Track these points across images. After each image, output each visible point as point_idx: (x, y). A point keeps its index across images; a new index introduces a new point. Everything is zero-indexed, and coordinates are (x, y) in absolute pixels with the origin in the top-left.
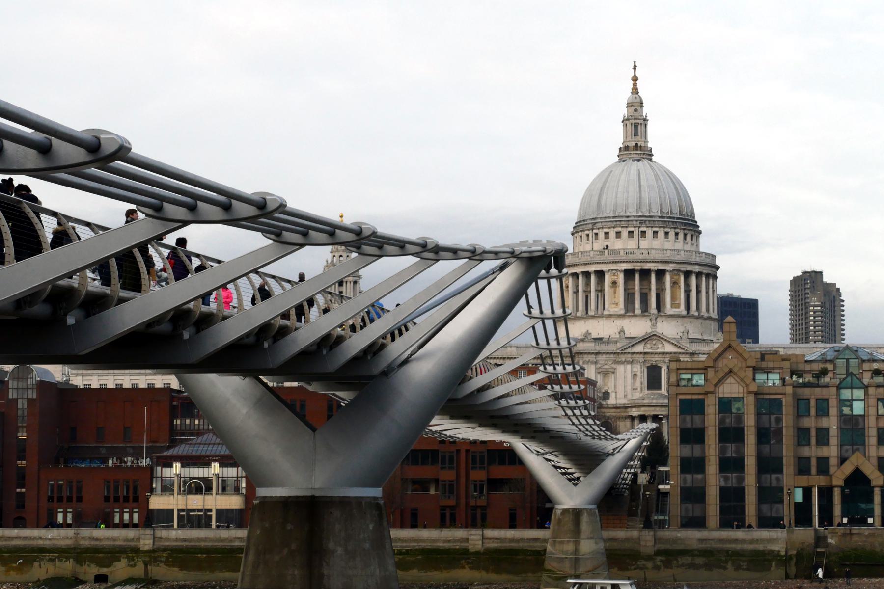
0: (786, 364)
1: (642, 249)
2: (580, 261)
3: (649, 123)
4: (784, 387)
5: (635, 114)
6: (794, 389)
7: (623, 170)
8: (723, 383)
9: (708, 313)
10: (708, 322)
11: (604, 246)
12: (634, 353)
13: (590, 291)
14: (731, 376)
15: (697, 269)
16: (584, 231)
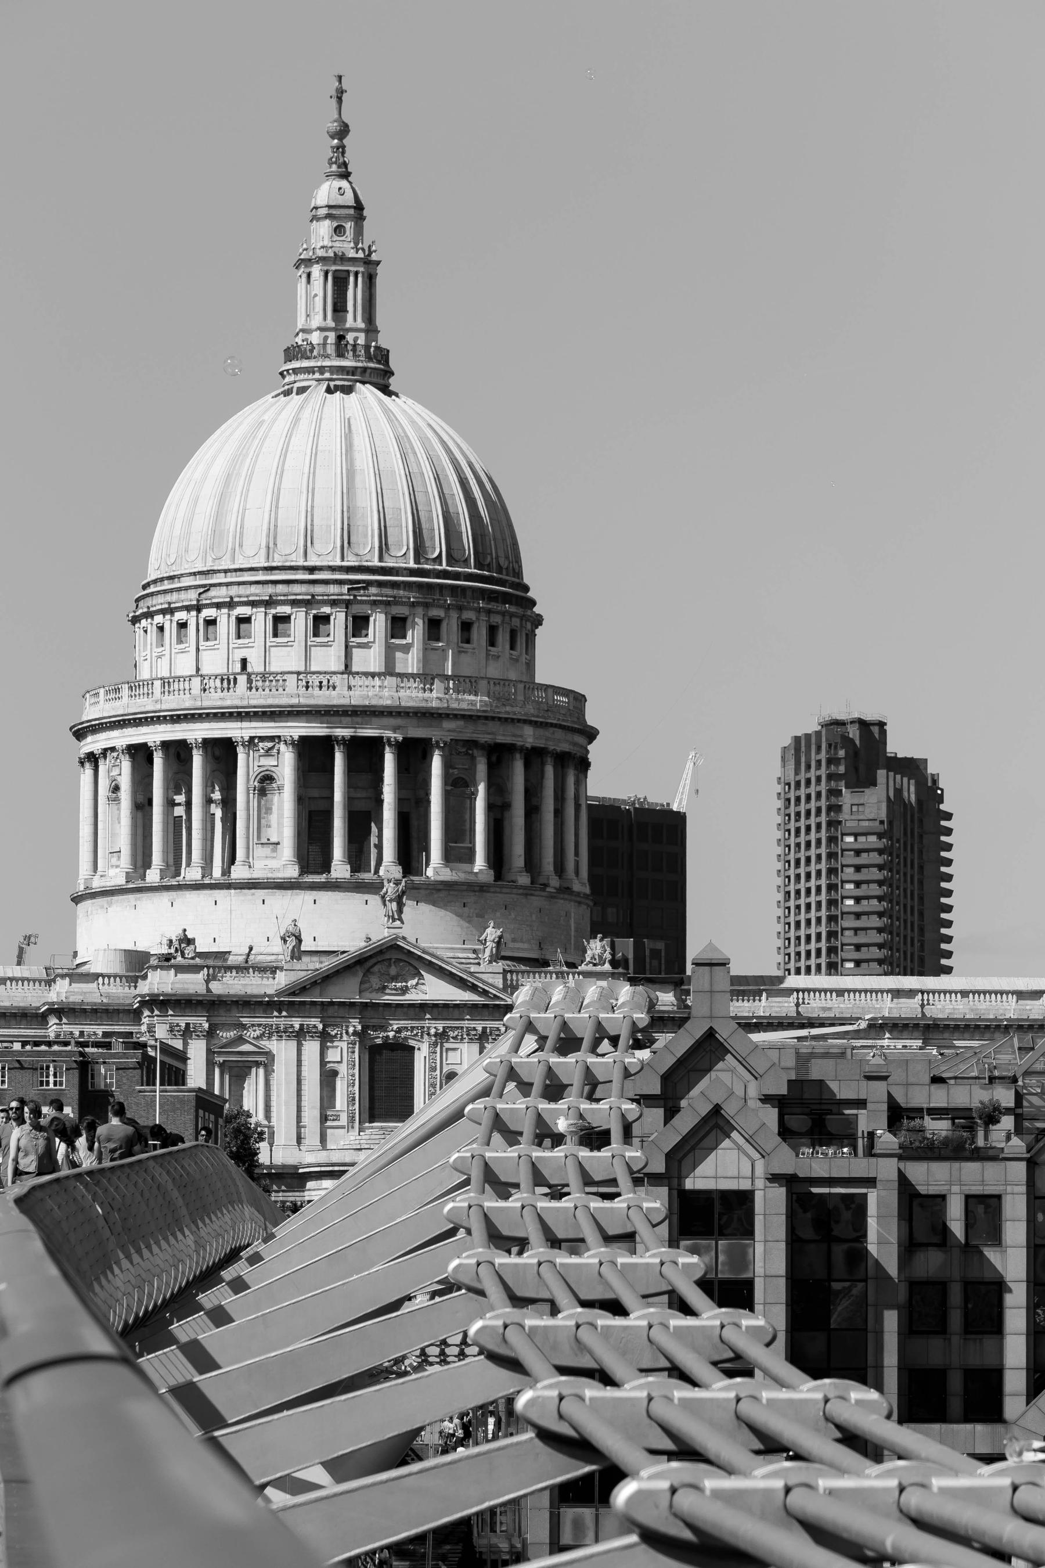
0: (877, 1092)
1: (358, 673)
2: (158, 707)
3: (380, 269)
4: (873, 1160)
5: (337, 244)
6: (902, 1165)
7: (296, 420)
8: (693, 1148)
9: (560, 877)
10: (563, 905)
11: (239, 655)
12: (332, 1003)
13: (188, 804)
14: (717, 1126)
15: (529, 737)
16: (170, 611)
